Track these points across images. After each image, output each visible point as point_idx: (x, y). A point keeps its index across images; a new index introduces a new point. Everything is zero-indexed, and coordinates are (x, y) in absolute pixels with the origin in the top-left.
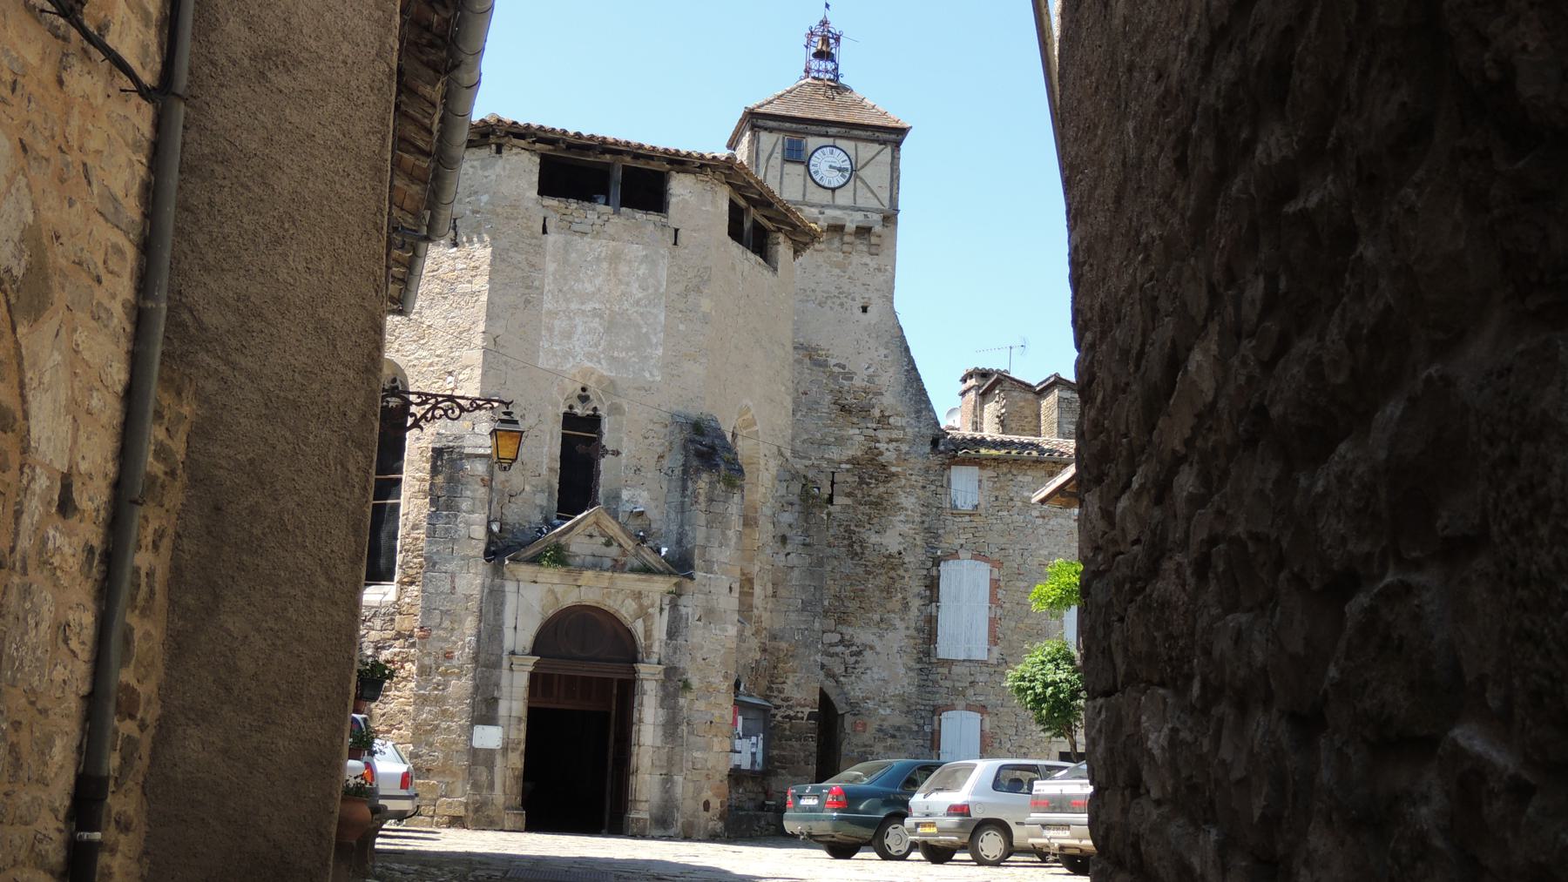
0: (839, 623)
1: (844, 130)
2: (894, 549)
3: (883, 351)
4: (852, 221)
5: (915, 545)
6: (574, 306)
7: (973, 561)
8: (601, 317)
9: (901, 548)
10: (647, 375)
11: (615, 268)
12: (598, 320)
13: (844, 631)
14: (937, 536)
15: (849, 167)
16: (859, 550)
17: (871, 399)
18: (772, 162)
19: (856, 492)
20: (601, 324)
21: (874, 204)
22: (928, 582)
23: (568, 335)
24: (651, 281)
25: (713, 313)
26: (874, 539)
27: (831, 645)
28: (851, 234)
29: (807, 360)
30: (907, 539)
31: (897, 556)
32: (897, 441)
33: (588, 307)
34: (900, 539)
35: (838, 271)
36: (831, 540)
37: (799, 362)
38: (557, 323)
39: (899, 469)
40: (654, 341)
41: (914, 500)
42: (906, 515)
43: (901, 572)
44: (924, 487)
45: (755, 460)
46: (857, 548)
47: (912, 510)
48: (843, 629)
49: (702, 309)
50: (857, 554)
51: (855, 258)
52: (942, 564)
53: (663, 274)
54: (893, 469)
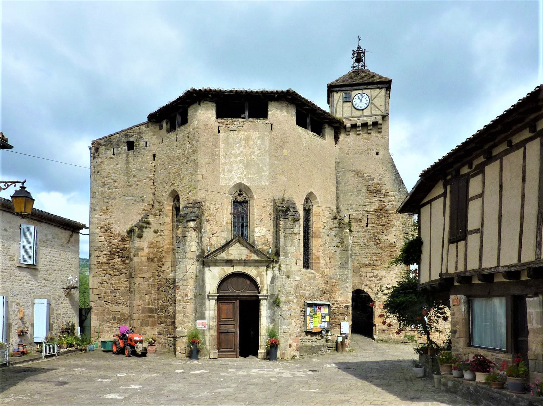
2: (392, 241)
3: (385, 169)
4: (370, 120)
6: (232, 160)
8: (243, 163)
9: (395, 240)
10: (263, 183)
11: (248, 143)
12: (242, 164)
16: (379, 242)
18: (339, 104)
20: (243, 165)
21: (379, 112)
23: (230, 171)
24: (262, 146)
25: (289, 155)
26: (384, 238)
27: (370, 277)
33: (238, 159)
34: (394, 237)
35: (366, 141)
36: (368, 240)
38: (226, 167)
40: (265, 169)
41: (399, 222)
42: (397, 228)
43: (395, 249)
45: (318, 212)
49: (284, 154)
50: (378, 244)
53: (267, 143)
54: (391, 212)
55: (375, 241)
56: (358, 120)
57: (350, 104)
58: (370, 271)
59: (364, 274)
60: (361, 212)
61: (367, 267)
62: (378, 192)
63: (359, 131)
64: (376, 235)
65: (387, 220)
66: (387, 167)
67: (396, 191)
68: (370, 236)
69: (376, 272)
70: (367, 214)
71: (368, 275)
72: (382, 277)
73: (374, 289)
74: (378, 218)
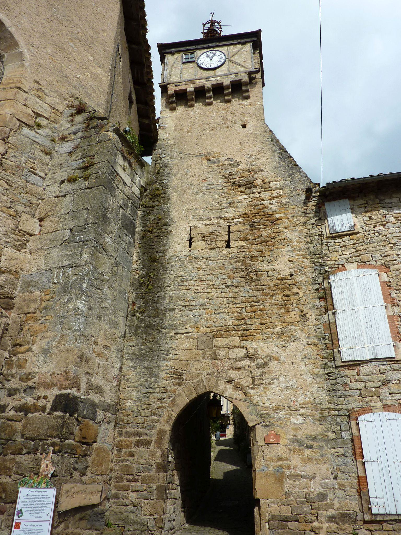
2: (286, 272)
9: (292, 271)
15: (224, 57)
16: (255, 277)
19: (248, 236)
22: (321, 294)
26: (267, 267)
29: (205, 162)
31: (289, 277)
34: (290, 263)
35: (223, 111)
36: (231, 273)
39: (282, 215)
41: (298, 234)
42: (292, 246)
43: (296, 290)
44: (304, 223)
52: (331, 277)
54: (277, 216)
55: (248, 275)
57: (194, 64)
58: (238, 344)
59: (222, 353)
60: (215, 221)
61: (230, 335)
62: (250, 185)
63: (210, 98)
64: (247, 262)
65: (269, 231)
67: (284, 180)
68: (234, 265)
69: (251, 345)
70: (228, 224)
71: (234, 353)
72: (269, 358)
73: (250, 391)
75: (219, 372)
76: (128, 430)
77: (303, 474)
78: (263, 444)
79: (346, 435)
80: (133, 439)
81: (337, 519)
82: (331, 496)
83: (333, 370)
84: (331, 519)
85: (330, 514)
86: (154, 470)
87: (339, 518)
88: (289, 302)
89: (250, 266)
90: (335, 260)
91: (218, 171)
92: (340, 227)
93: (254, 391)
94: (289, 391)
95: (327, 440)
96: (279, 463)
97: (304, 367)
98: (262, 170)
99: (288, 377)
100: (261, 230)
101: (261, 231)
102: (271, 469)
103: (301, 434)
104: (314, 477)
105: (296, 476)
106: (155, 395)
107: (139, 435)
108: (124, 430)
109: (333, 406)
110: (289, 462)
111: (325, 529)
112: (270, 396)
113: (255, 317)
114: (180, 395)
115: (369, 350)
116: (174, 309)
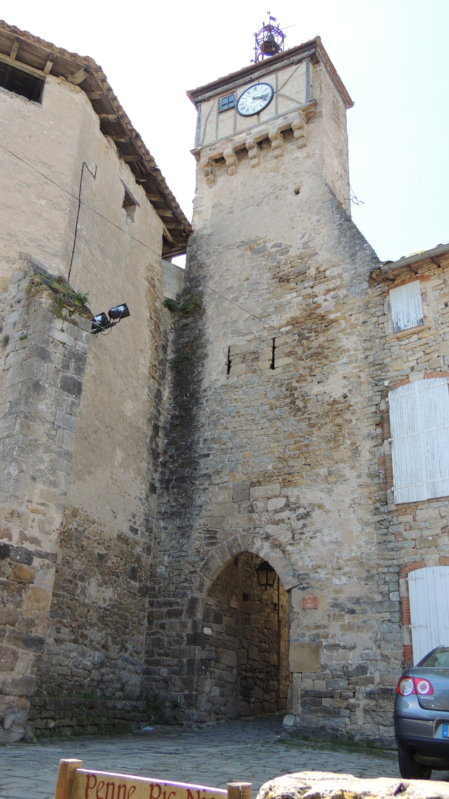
0: (284, 486)
1: (264, 70)
2: (337, 394)
3: (315, 218)
5: (361, 384)
7: (426, 380)
9: (346, 391)
13: (289, 494)
14: (382, 366)
17: (306, 262)
22: (378, 419)
26: (316, 389)
27: (276, 512)
28: (276, 138)
29: (248, 253)
30: (352, 380)
31: (342, 400)
32: (334, 289)
34: (345, 382)
35: (273, 174)
36: (274, 401)
37: (242, 256)
39: (339, 314)
41: (355, 338)
42: (349, 356)
46: (300, 403)
47: (355, 349)
48: (288, 491)
50: (299, 410)
51: (287, 158)
52: (390, 394)
54: (332, 316)
55: (293, 402)
56: (248, 135)
57: (232, 112)
59: (260, 505)
66: (319, 213)
70: (272, 337)
72: (313, 506)
73: (289, 548)
74: (300, 341)
75: (255, 528)
76: (159, 599)
77: (342, 644)
78: (299, 610)
79: (394, 597)
80: (164, 610)
81: (377, 696)
82: (371, 669)
83: (385, 517)
84: (370, 695)
85: (369, 689)
86: (185, 642)
87: (378, 694)
88: (339, 433)
89: (296, 390)
90: (398, 370)
91: (264, 263)
92: (406, 323)
93: (294, 548)
94: (332, 546)
95: (373, 603)
96: (316, 632)
97: (353, 516)
98: (316, 254)
99: (332, 528)
100: (312, 339)
101: (312, 341)
102: (307, 638)
103: (342, 598)
104: (354, 648)
105: (335, 646)
106: (187, 559)
107: (170, 604)
108: (155, 600)
109: (382, 562)
110: (326, 630)
111: (362, 706)
112: (311, 552)
113: (299, 458)
114: (213, 557)
115: (428, 488)
116: (208, 455)
